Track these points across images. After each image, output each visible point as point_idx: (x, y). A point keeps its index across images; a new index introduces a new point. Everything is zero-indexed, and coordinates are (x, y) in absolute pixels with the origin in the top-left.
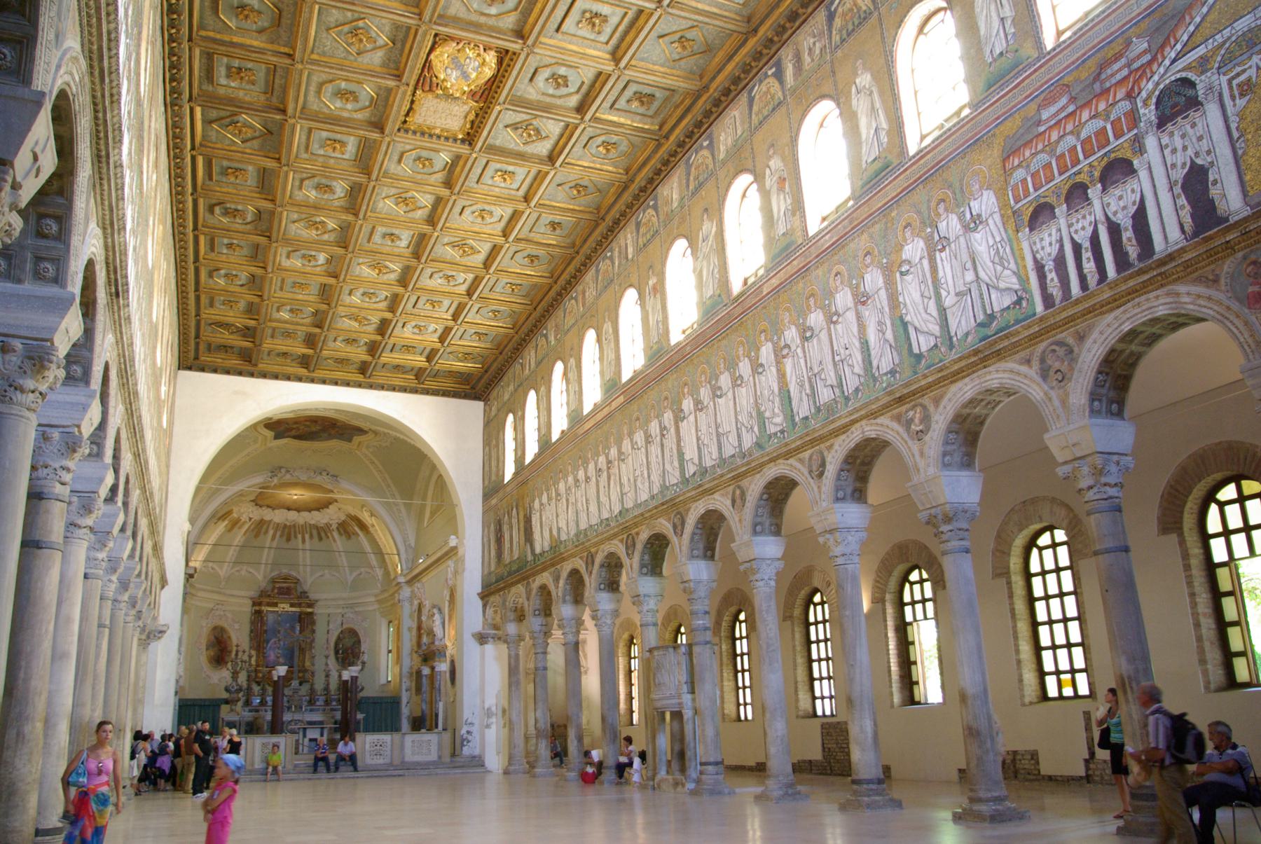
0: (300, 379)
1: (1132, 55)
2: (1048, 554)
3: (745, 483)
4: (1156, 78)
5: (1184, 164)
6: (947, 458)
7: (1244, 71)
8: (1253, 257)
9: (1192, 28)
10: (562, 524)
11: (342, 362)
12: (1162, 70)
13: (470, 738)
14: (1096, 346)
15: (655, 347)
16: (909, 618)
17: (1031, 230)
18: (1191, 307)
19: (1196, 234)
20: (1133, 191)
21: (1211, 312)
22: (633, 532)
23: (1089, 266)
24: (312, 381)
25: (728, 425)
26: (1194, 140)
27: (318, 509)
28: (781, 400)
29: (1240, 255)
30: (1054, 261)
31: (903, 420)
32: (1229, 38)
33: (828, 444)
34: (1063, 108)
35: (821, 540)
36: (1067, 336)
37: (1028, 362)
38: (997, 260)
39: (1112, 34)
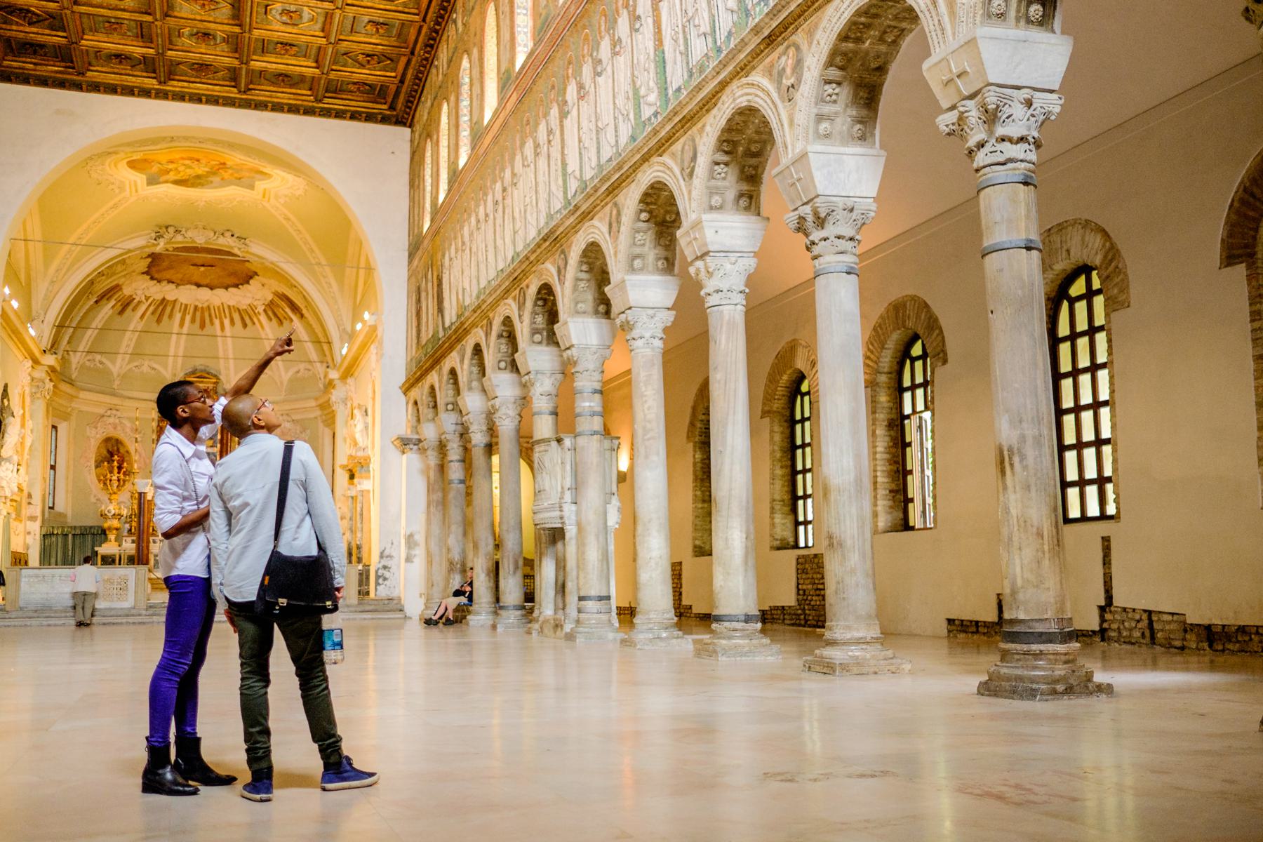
0: (146, 93)
2: (1081, 307)
3: (620, 199)
6: (824, 125)
10: (467, 286)
11: (202, 68)
13: (387, 574)
15: (544, 13)
16: (908, 410)
22: (524, 285)
24: (163, 95)
25: (607, 118)
27: (236, 286)
28: (656, 67)
31: (775, 72)
33: (699, 125)
35: (692, 270)
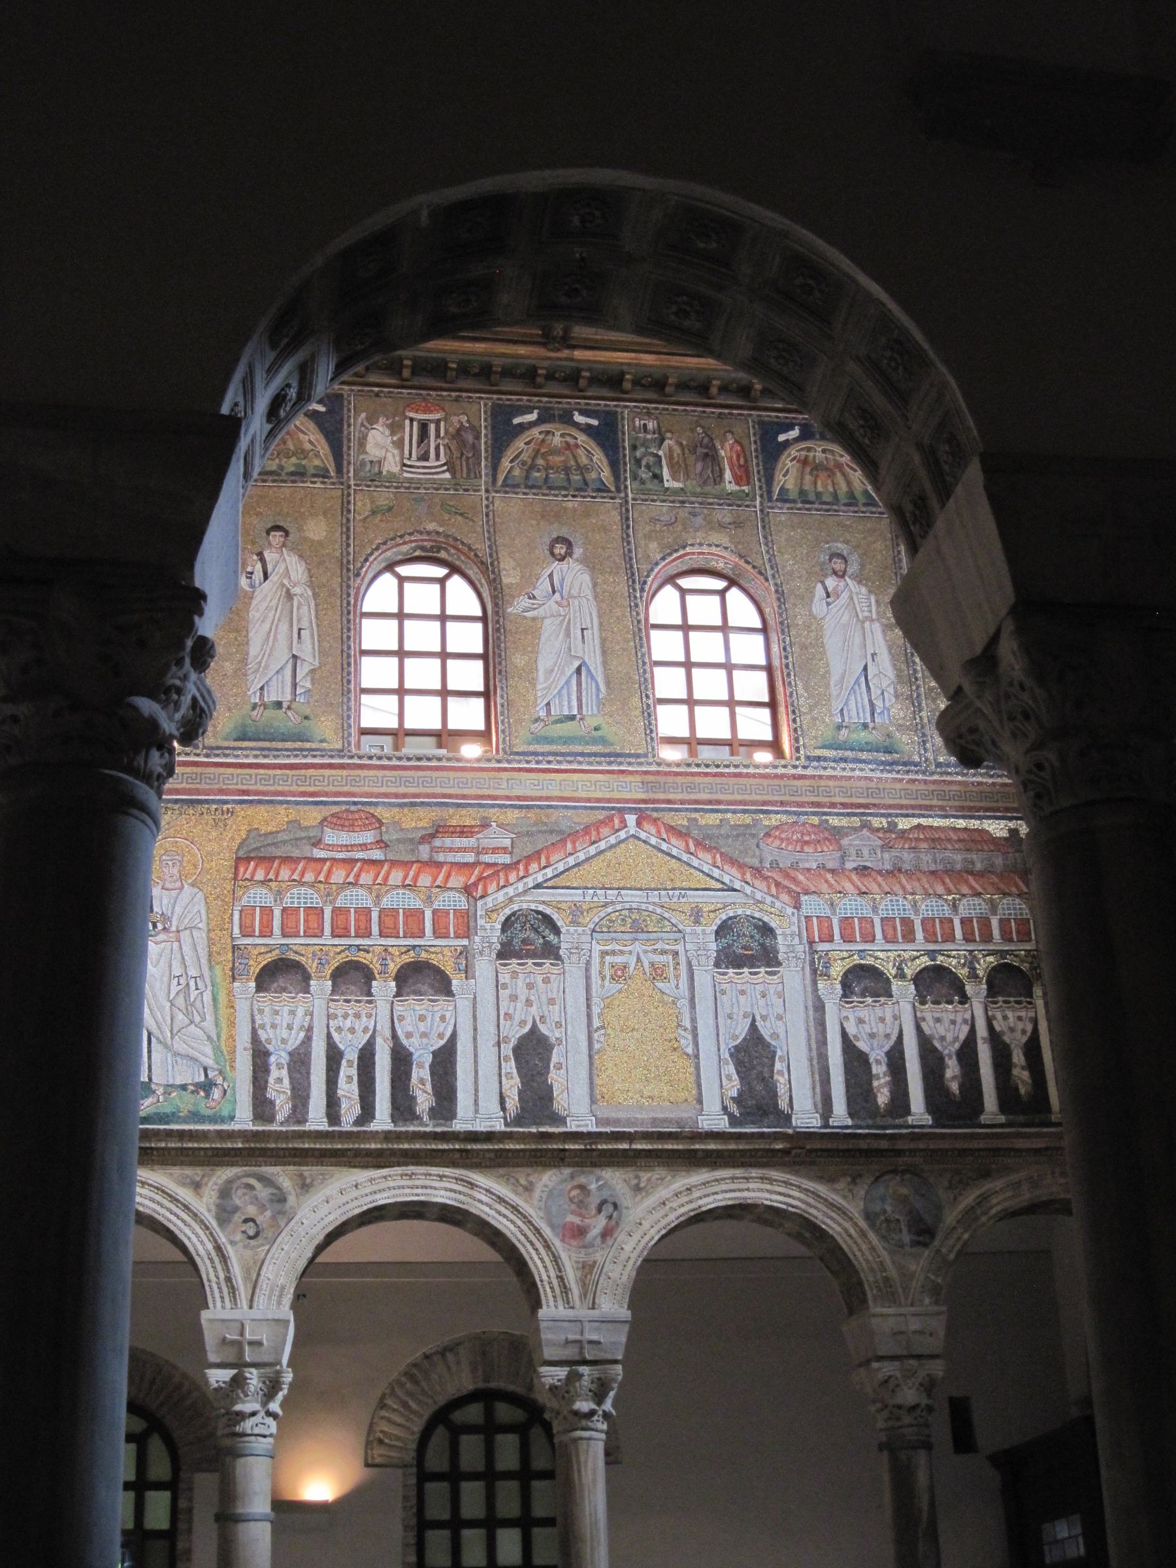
1: (486, 843)
4: (510, 891)
5: (523, 1023)
7: (622, 952)
8: (582, 1180)
9: (571, 861)
12: (520, 886)
14: (325, 1209)
17: (260, 988)
18: (487, 1209)
19: (518, 1120)
20: (443, 1018)
21: (512, 1227)
23: (348, 1088)
26: (544, 999)
29: (567, 1171)
30: (290, 1054)
32: (612, 903)
34: (364, 847)
36: (283, 1176)
37: (197, 1186)
38: (180, 1002)
39: (464, 797)
